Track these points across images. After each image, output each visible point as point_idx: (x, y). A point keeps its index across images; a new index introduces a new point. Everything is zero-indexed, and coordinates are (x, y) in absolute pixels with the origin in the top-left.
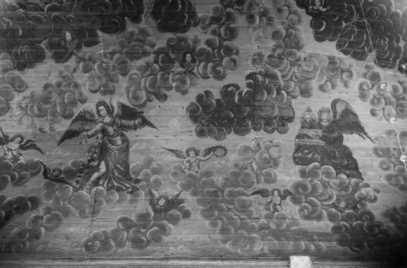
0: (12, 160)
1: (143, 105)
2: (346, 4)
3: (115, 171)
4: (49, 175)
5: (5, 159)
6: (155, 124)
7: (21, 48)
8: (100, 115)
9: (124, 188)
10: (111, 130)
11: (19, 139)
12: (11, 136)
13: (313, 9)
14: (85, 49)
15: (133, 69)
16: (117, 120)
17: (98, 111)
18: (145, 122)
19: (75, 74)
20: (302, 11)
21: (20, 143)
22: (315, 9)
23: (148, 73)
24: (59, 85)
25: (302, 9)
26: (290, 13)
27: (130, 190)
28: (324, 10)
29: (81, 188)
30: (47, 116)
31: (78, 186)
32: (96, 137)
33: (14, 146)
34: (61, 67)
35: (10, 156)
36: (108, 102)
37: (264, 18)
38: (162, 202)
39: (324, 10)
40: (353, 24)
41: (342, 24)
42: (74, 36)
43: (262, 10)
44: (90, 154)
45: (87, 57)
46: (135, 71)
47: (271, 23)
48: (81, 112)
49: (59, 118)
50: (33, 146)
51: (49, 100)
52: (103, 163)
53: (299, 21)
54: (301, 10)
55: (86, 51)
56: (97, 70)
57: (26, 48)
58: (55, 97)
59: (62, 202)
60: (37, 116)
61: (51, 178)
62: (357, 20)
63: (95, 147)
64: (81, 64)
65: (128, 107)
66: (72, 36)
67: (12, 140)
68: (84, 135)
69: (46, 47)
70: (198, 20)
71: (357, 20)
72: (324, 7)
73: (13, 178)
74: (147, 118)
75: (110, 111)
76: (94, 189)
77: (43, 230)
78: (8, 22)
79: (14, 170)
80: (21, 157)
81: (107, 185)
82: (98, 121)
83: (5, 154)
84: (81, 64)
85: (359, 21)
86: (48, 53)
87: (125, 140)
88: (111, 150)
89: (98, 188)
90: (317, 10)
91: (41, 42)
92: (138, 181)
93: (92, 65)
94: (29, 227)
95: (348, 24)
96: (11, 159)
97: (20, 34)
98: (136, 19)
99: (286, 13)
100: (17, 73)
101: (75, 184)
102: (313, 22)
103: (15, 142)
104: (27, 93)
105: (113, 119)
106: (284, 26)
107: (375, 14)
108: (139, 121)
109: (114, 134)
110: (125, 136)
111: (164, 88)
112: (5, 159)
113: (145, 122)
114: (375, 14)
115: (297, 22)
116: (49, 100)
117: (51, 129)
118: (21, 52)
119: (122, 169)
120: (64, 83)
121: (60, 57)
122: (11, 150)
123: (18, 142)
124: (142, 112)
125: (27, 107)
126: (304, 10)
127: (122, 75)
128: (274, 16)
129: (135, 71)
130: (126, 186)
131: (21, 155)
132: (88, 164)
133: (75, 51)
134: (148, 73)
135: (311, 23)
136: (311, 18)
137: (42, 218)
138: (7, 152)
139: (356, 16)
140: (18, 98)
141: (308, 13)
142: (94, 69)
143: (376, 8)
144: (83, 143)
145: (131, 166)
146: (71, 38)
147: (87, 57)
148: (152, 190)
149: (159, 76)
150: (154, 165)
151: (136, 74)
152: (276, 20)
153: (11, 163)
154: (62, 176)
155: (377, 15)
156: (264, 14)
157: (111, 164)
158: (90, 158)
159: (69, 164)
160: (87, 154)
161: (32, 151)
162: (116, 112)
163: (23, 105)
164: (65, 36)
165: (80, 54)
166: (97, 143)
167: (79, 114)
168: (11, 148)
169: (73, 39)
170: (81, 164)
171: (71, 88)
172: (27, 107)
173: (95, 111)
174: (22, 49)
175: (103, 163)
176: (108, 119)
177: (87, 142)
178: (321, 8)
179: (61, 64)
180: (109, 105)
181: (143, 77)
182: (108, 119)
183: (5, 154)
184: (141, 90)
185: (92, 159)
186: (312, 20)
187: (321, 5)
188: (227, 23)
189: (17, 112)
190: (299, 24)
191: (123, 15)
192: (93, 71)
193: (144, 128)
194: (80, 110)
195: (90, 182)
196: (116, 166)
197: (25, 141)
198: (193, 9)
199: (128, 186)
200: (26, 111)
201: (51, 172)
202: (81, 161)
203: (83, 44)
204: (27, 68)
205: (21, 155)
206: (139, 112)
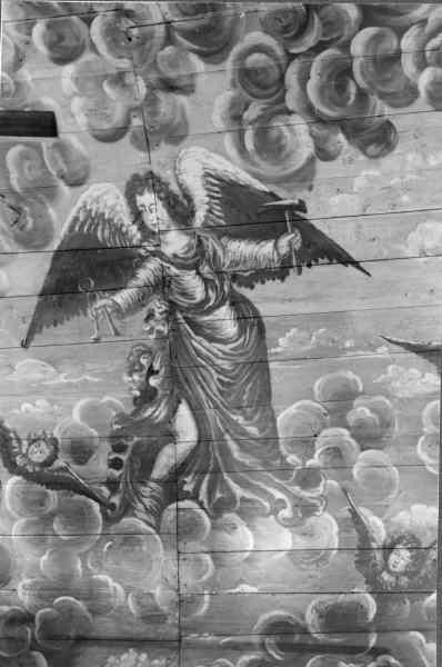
1: (305, 176)
3: (227, 437)
4: (19, 460)
6: (355, 255)
8: (142, 227)
9: (267, 504)
10: (194, 284)
15: (248, 31)
16: (211, 243)
17: (137, 216)
18: (320, 250)
19: (26, 74)
23: (310, 40)
27: (286, 513)
29: (127, 508)
32: (144, 313)
36: (166, 175)
38: (401, 559)
44: (136, 377)
46: (256, 37)
48: (76, 219)
52: (184, 409)
56: (102, 47)
61: (30, 470)
63: (149, 352)
64: (39, 29)
65: (246, 187)
74: (319, 225)
75: (181, 210)
76: (170, 513)
81: (211, 492)
82: (142, 251)
87: (249, 318)
88: (207, 359)
89: (182, 504)
92: (309, 478)
93: (83, 26)
101: (106, 491)
105: (194, 242)
108: (290, 244)
109: (207, 299)
110: (247, 301)
111: (382, 96)
113: (320, 250)
119: (253, 430)
124: (302, 206)
127: (203, 55)
129: (256, 37)
130: (270, 497)
132: (135, 413)
134: (310, 40)
142: (93, 48)
145: (280, 419)
148: (363, 512)
149: (358, 46)
150: (361, 411)
151: (258, 49)
157: (210, 412)
158: (138, 393)
159: (76, 417)
160: (126, 378)
162: (200, 216)
166: (152, 337)
167: (71, 228)
170: (114, 414)
173: (124, 217)
175: (184, 409)
176: (176, 243)
180: (174, 187)
181: (291, 57)
182: (176, 243)
184: (290, 113)
185: (147, 396)
192: (88, 56)
193: (315, 269)
194: (73, 213)
195: (152, 485)
196: (229, 420)
199: (279, 495)
201: (25, 443)
202: (111, 405)
206: (291, 208)
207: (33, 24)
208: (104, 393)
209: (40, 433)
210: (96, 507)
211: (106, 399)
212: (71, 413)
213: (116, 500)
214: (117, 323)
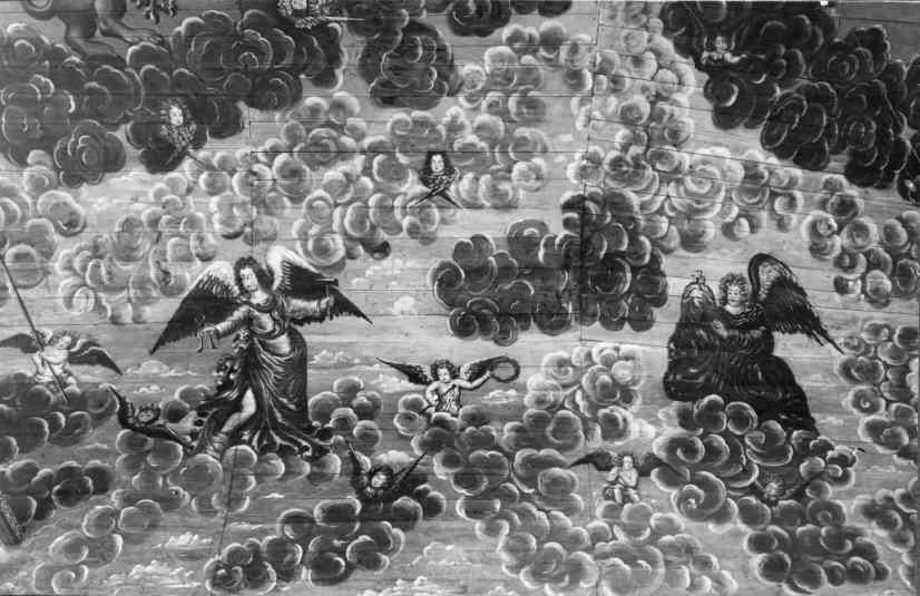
0: (52, 386)
1: (339, 266)
2: (783, 50)
3: (275, 410)
4: (131, 421)
5: (37, 383)
6: (363, 311)
7: (73, 140)
8: (241, 287)
9: (296, 448)
10: (266, 320)
11: (67, 339)
12: (49, 333)
13: (710, 58)
14: (211, 142)
15: (317, 188)
16: (281, 300)
17: (239, 280)
18: (344, 307)
19: (190, 199)
20: (686, 67)
21: (68, 348)
22: (715, 58)
23: (348, 197)
24: (154, 222)
25: (687, 57)
26: (660, 67)
27: (309, 453)
28: (736, 60)
29: (202, 448)
30: (128, 289)
31: (195, 444)
32: (234, 336)
33: (57, 355)
34: (161, 181)
35: (47, 377)
36: (259, 259)
37: (602, 77)
38: (379, 480)
39: (736, 60)
40: (798, 91)
41: (774, 91)
42: (189, 116)
43: (599, 59)
44: (221, 373)
45: (215, 162)
46: (320, 192)
47: (618, 87)
48: (201, 281)
49: (155, 294)
50: (102, 359)
51: (134, 254)
52: (249, 394)
53: (681, 83)
54: (685, 60)
55: (215, 151)
56: (237, 189)
57: (83, 141)
58: (145, 245)
59: (160, 481)
60: (107, 289)
61: (137, 425)
62: (806, 82)
63: (232, 359)
64: (204, 176)
65: (306, 270)
66: (184, 115)
67: (51, 342)
68: (208, 332)
69: (128, 138)
70: (459, 82)
71: (806, 82)
72: (735, 54)
73: (54, 425)
74: (345, 294)
75: (265, 278)
76: (231, 452)
77: (119, 540)
78: (46, 86)
79: (55, 408)
80: (71, 380)
81: (260, 441)
82: (239, 301)
83: (38, 373)
84: (204, 176)
85: (812, 84)
86: (132, 151)
87: (297, 341)
88: (269, 365)
89: (241, 447)
90: (718, 60)
91: (115, 126)
92: (326, 434)
93: (228, 177)
94: (87, 534)
95: (786, 91)
96: (49, 383)
97: (71, 111)
98: (325, 79)
99: (651, 62)
100: (64, 195)
101: (189, 439)
102: (710, 86)
103: (58, 345)
104: (85, 240)
105: (271, 298)
106: (647, 93)
107: (847, 70)
108: (327, 303)
109: (274, 330)
110: (297, 332)
111: (384, 228)
112: (37, 383)
113: (344, 307)
114: (847, 70)
115: (676, 86)
116: (134, 254)
117: (137, 320)
118: (74, 151)
119: (292, 407)
120: (165, 218)
121: (161, 157)
122: (49, 363)
123: (65, 346)
124: (336, 283)
125: (84, 269)
126: (691, 60)
127: (292, 200)
128: (623, 72)
129: (320, 192)
130: (299, 445)
131: (70, 374)
132: (218, 394)
133: (191, 151)
134: (348, 197)
135: (706, 89)
136: (706, 77)
137: (116, 514)
138: (41, 369)
139: (806, 73)
140: (65, 249)
141: (699, 66)
142: (232, 189)
143: (851, 55)
144: (205, 350)
145: (311, 402)
146: (181, 119)
147: (215, 162)
148: (357, 453)
149: (372, 202)
150: (361, 398)
151: (321, 198)
152: (628, 82)
153: (48, 392)
154: (160, 422)
155: (850, 73)
156: (601, 69)
157: (266, 395)
158: (220, 383)
159: (177, 396)
160: (215, 374)
161: (99, 370)
162: (277, 284)
163: (77, 266)
164: (168, 115)
165: (201, 154)
166: (236, 350)
167: (197, 286)
168: (51, 359)
169: (186, 123)
171: (181, 229)
172: (84, 269)
173: (231, 281)
174: (76, 143)
175: (249, 394)
176: (260, 297)
177: (214, 347)
178: (728, 56)
179: (159, 176)
180: (264, 267)
181: (337, 205)
182: (260, 297)
183: (38, 373)
184: (334, 233)
185: (227, 385)
186: (708, 83)
187: (727, 50)
188: (522, 88)
189: (64, 282)
190: (679, 91)
191: (296, 70)
192: (228, 193)
193: (340, 317)
194: (200, 277)
195: (222, 435)
196: (278, 401)
197: (80, 343)
198: (450, 58)
199: (304, 443)
200: (84, 278)
201: (137, 411)
202: (202, 390)
203: (207, 133)
204: (85, 184)
205: (70, 374)
206: (329, 282)
207: (202, 172)
208: (197, 383)
209: (149, 405)
210: (180, 447)
211: (200, 386)
212: (173, 394)
213: (195, 444)
214: (215, 341)
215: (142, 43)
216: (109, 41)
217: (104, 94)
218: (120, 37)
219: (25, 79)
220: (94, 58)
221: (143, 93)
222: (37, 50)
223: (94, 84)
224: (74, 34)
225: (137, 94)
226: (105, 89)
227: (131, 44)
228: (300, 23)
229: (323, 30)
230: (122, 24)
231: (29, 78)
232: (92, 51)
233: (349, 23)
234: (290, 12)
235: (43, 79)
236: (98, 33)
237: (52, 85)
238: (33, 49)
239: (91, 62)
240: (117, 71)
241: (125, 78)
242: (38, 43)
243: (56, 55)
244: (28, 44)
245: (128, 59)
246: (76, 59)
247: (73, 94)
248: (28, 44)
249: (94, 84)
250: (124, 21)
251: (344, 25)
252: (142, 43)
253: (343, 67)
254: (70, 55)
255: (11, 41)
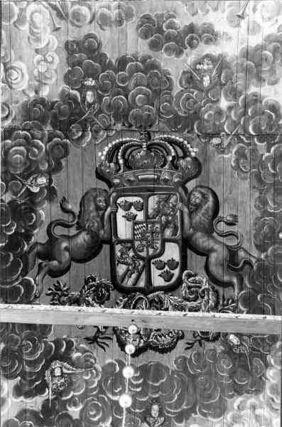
78: (11, 230)
98: (18, 391)
191: (23, 374)
215: (35, 286)
216: (36, 268)
217: (7, 263)
218: (38, 274)
219: (13, 219)
220: (27, 259)
221: (8, 287)
222: (30, 226)
223: (12, 258)
224: (39, 248)
225: (7, 283)
226: (9, 264)
227: (35, 280)
228: (48, 373)
229: (44, 386)
230: (45, 275)
231: (14, 220)
232: (31, 257)
233: (48, 400)
234: (53, 367)
235: (14, 228)
236: (40, 261)
237: (10, 233)
238: (31, 224)
239: (24, 256)
240: (19, 272)
241: (15, 277)
242: (34, 227)
243: (28, 237)
244: (34, 221)
245: (26, 278)
246: (26, 248)
247: (5, 246)
248: (34, 221)
249: (12, 258)
250: (47, 276)
251: (47, 397)
252: (35, 286)
253: (24, 400)
254: (28, 244)
255: (35, 212)
